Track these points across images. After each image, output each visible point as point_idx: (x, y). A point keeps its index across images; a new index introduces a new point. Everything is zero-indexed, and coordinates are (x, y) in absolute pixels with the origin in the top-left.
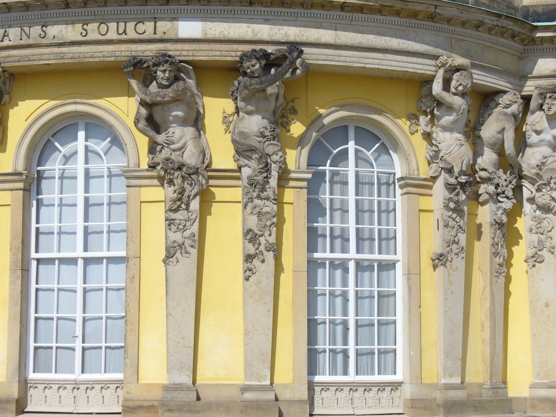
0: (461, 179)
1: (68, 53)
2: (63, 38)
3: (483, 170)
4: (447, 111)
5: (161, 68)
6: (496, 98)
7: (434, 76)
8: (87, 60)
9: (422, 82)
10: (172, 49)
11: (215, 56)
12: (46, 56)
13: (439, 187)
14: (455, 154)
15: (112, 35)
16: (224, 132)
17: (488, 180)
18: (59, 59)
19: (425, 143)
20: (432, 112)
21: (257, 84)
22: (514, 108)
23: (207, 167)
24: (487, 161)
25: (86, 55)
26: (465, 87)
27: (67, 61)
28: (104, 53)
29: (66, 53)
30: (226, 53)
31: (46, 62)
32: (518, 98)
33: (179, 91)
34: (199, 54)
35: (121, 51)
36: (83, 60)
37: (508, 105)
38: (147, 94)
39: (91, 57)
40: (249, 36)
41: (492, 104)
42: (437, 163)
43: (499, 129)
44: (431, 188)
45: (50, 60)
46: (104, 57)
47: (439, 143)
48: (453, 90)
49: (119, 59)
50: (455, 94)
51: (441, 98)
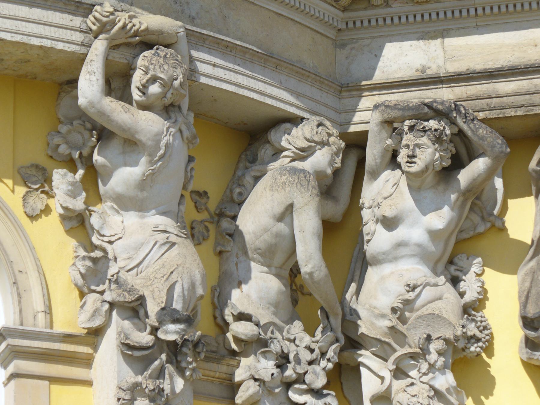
0: (167, 332)
3: (242, 317)
4: (124, 153)
6: (273, 136)
7: (81, 59)
9: (61, 84)
13: (108, 355)
14: (150, 270)
17: (258, 345)
19: (72, 243)
20: (87, 161)
22: (321, 159)
24: (254, 296)
26: (167, 85)
32: (329, 135)
37: (302, 150)
41: (265, 152)
42: (102, 293)
43: (279, 209)
44: (87, 362)
47: (111, 243)
48: (136, 95)
50: (143, 107)
51: (102, 113)
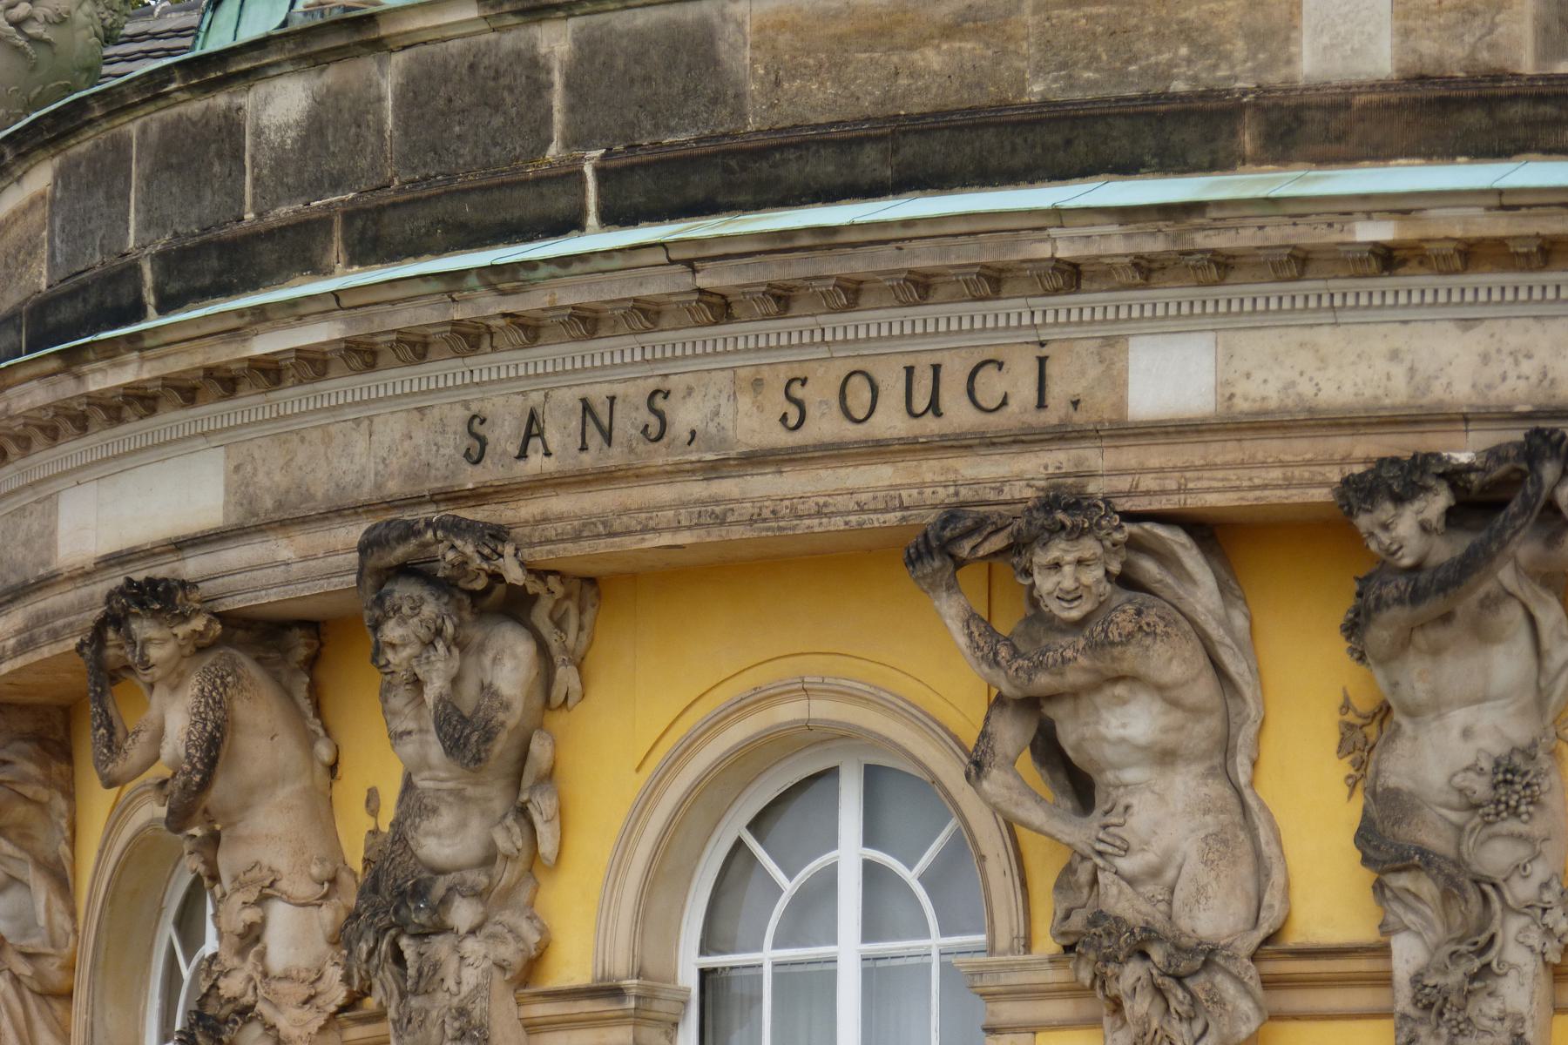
1: (737, 501)
5: (1042, 557)
10: (1106, 470)
11: (1265, 487)
15: (890, 421)
16: (1347, 790)
21: (1399, 601)
23: (1268, 940)
27: (738, 533)
28: (864, 497)
30: (1305, 473)
31: (666, 539)
33: (1113, 644)
34: (1205, 484)
35: (922, 486)
38: (997, 664)
39: (819, 514)
40: (1397, 391)
45: (678, 528)
46: (861, 509)
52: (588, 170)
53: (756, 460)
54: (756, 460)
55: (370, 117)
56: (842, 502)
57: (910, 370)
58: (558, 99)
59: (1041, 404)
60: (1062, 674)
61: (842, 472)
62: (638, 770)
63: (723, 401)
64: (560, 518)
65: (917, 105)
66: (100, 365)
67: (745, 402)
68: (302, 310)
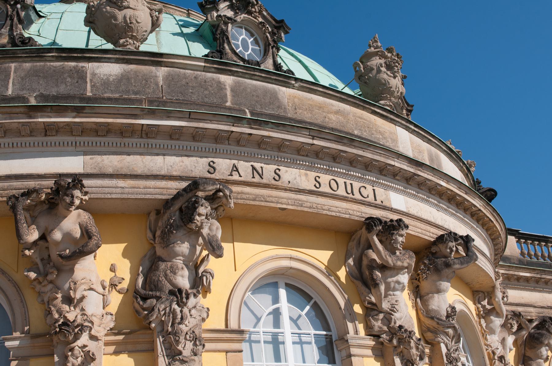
2: (299, 186)
8: (325, 212)
12: (285, 200)
18: (297, 206)
25: (324, 208)
27: (306, 209)
28: (340, 209)
29: (304, 201)
31: (284, 206)
35: (354, 210)
36: (321, 212)
39: (329, 210)
45: (288, 204)
49: (353, 217)
52: (247, 111)
53: (311, 192)
54: (311, 192)
55: (152, 80)
56: (334, 209)
57: (345, 183)
58: (229, 93)
59: (376, 200)
60: (403, 262)
61: (334, 202)
62: (235, 270)
63: (297, 176)
64: (248, 194)
65: (331, 125)
66: (50, 114)
67: (303, 178)
68: (172, 115)
